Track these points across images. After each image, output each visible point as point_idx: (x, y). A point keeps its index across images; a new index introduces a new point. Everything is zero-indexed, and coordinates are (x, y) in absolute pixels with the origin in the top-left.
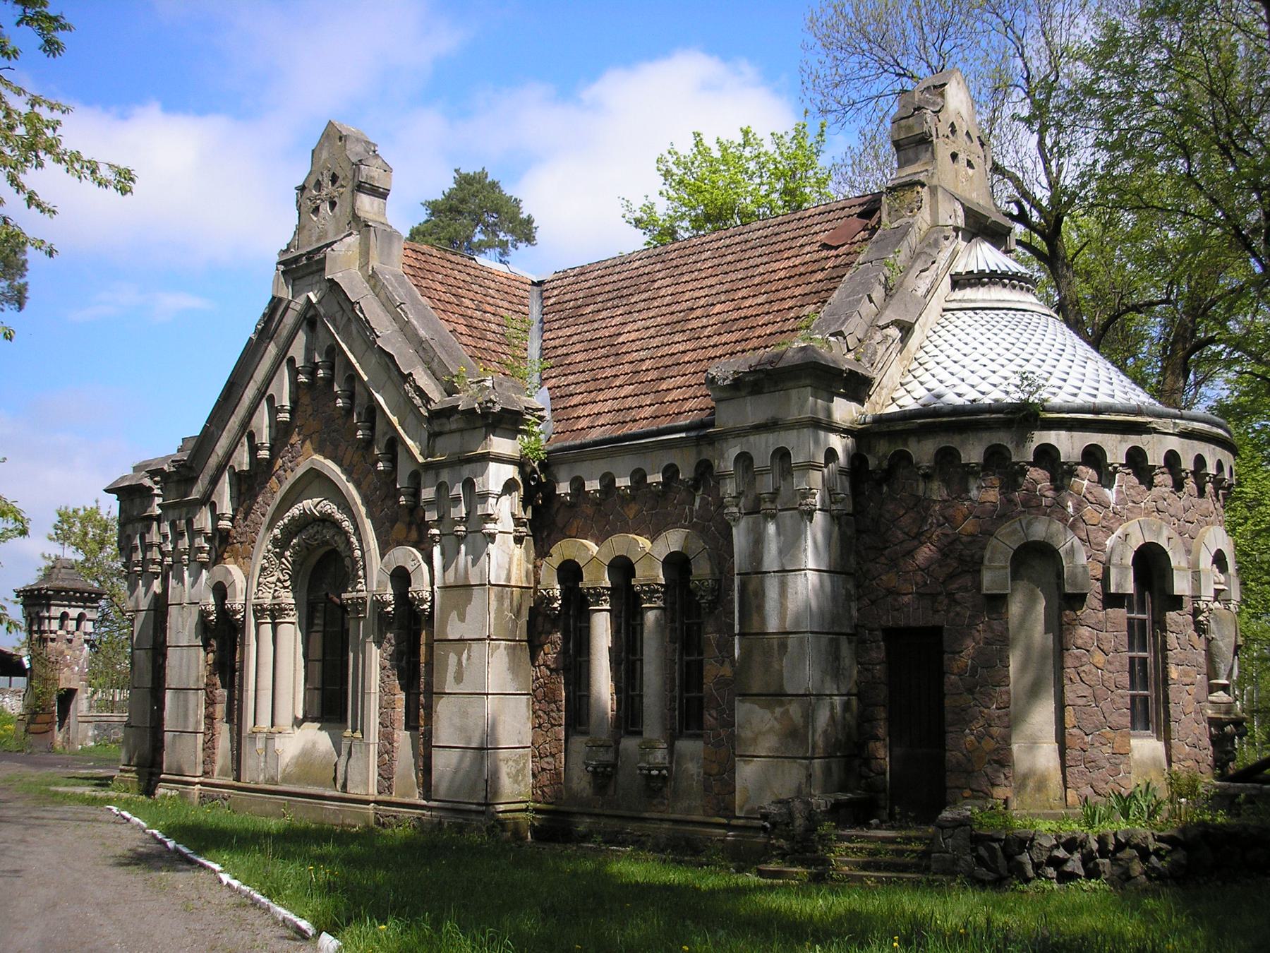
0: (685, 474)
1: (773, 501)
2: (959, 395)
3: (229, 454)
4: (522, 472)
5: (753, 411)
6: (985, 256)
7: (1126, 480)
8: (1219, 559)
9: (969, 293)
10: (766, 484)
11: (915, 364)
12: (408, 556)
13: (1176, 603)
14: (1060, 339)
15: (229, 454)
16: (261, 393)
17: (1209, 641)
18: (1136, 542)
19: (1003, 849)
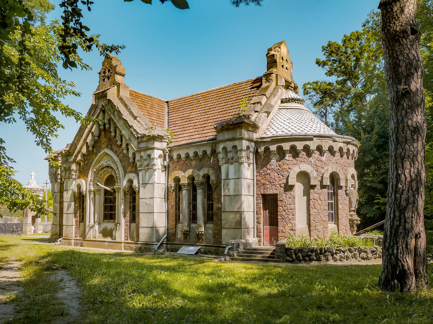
0: (209, 152)
1: (232, 160)
2: (283, 132)
3: (81, 148)
4: (164, 152)
5: (227, 135)
6: (291, 94)
7: (327, 155)
8: (353, 176)
9: (286, 104)
10: (230, 155)
11: (271, 123)
12: (132, 176)
13: (341, 187)
14: (311, 117)
15: (81, 148)
16: (90, 131)
17: (350, 198)
18: (330, 171)
19: (294, 252)
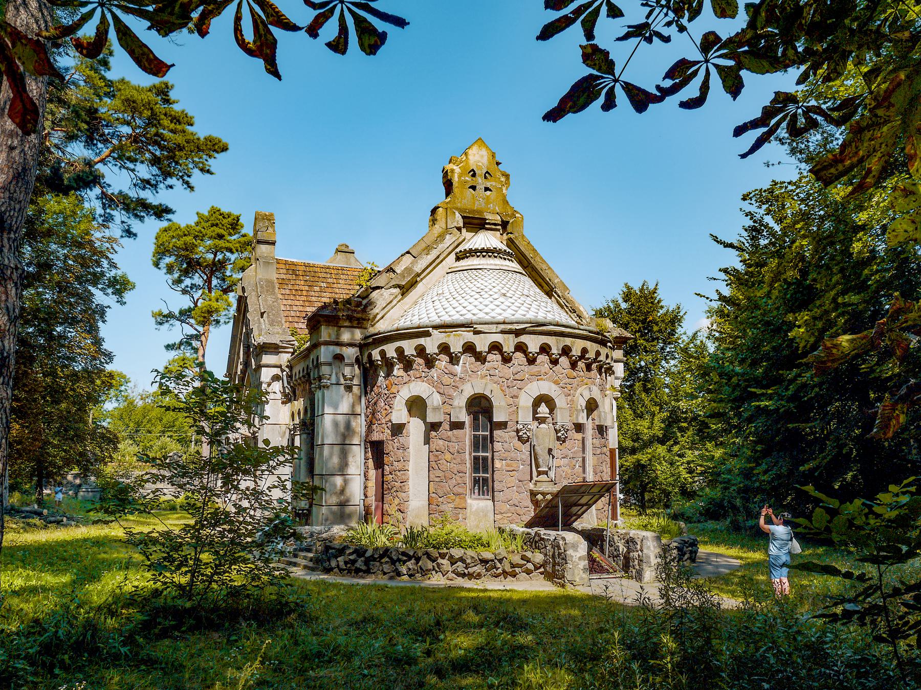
7: (467, 360)
